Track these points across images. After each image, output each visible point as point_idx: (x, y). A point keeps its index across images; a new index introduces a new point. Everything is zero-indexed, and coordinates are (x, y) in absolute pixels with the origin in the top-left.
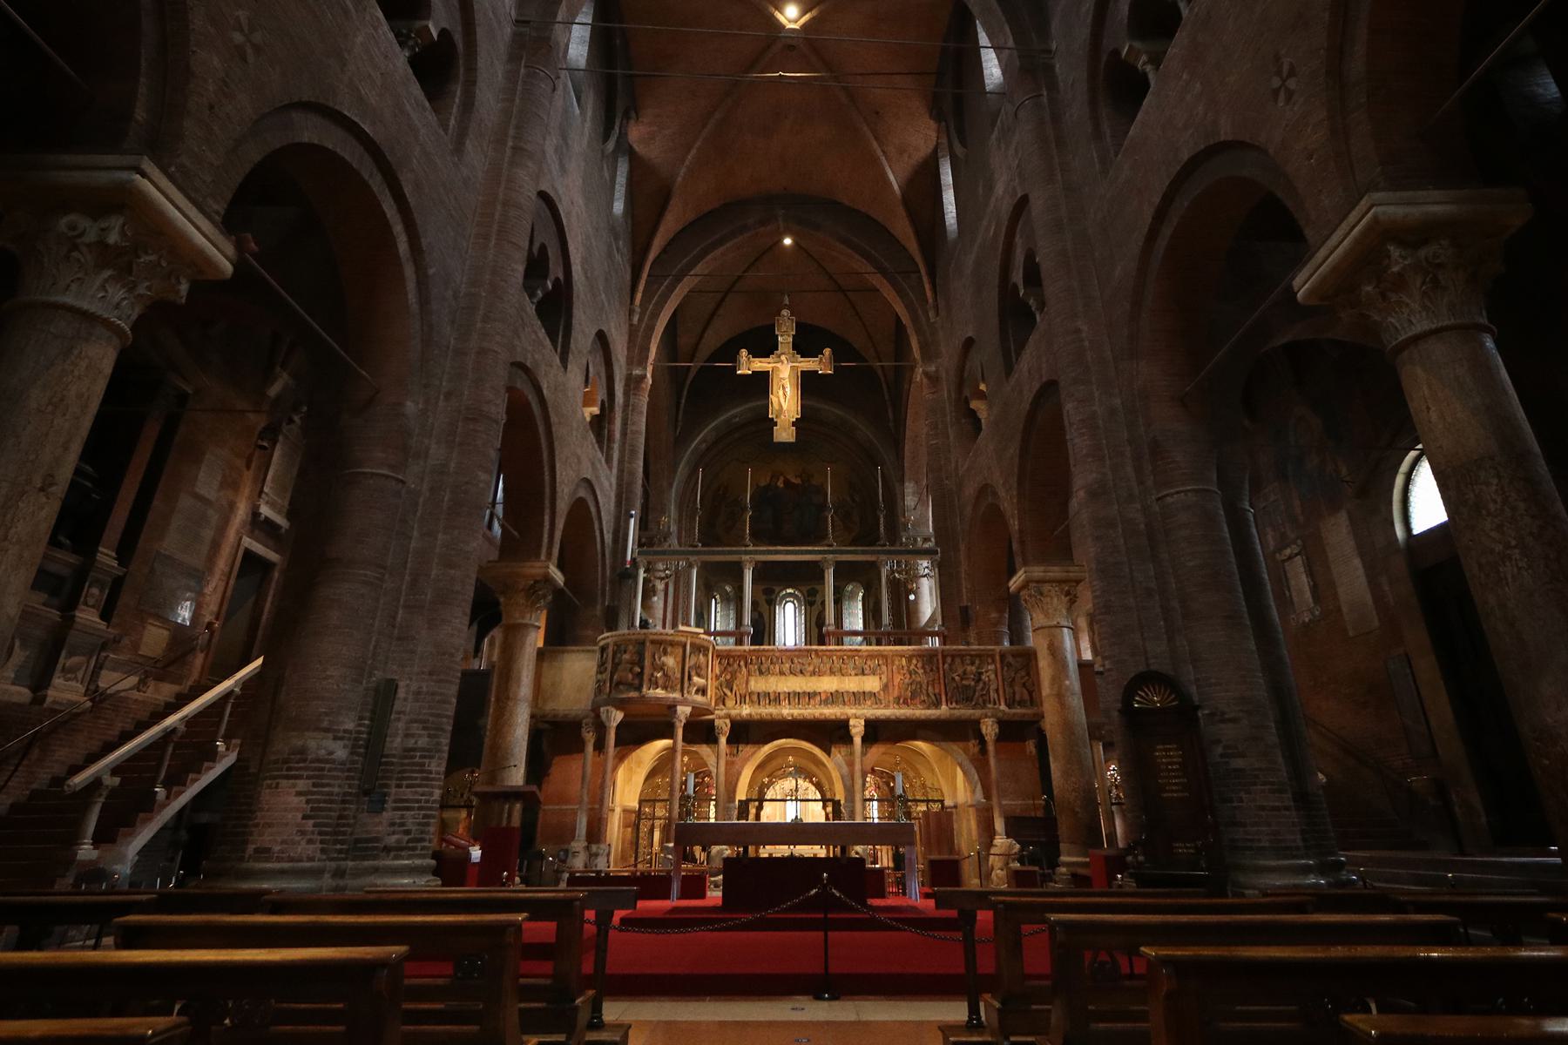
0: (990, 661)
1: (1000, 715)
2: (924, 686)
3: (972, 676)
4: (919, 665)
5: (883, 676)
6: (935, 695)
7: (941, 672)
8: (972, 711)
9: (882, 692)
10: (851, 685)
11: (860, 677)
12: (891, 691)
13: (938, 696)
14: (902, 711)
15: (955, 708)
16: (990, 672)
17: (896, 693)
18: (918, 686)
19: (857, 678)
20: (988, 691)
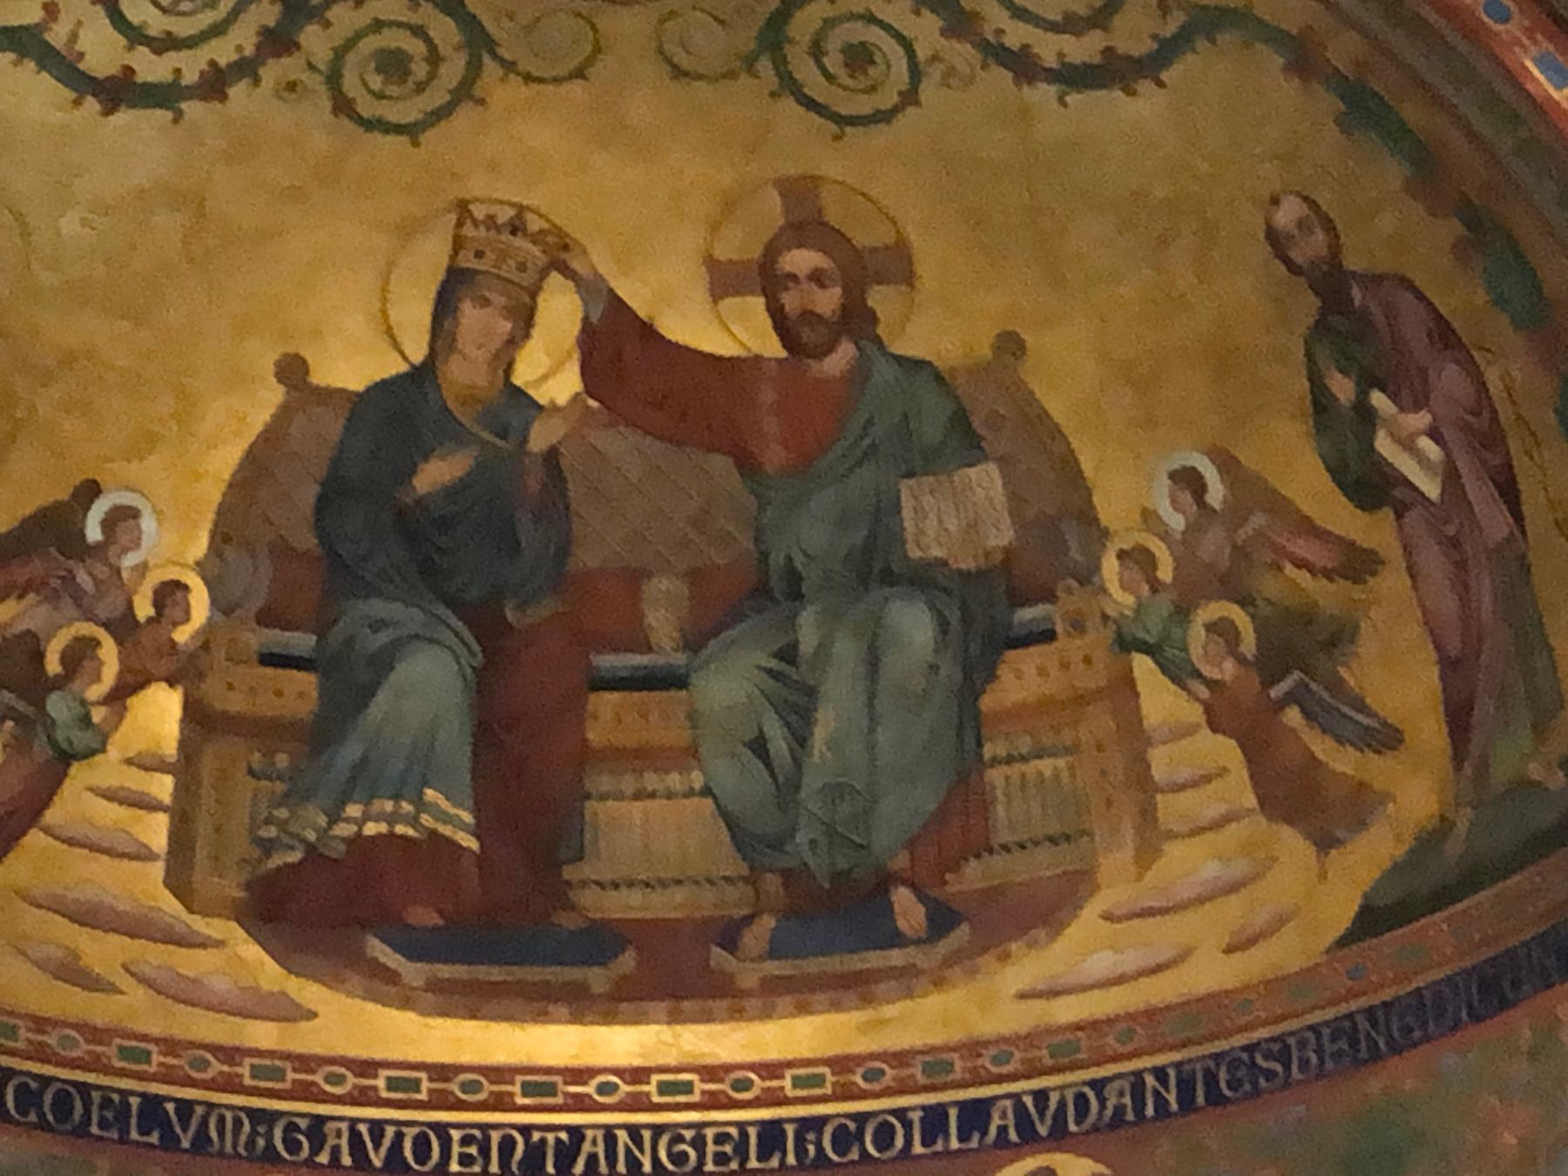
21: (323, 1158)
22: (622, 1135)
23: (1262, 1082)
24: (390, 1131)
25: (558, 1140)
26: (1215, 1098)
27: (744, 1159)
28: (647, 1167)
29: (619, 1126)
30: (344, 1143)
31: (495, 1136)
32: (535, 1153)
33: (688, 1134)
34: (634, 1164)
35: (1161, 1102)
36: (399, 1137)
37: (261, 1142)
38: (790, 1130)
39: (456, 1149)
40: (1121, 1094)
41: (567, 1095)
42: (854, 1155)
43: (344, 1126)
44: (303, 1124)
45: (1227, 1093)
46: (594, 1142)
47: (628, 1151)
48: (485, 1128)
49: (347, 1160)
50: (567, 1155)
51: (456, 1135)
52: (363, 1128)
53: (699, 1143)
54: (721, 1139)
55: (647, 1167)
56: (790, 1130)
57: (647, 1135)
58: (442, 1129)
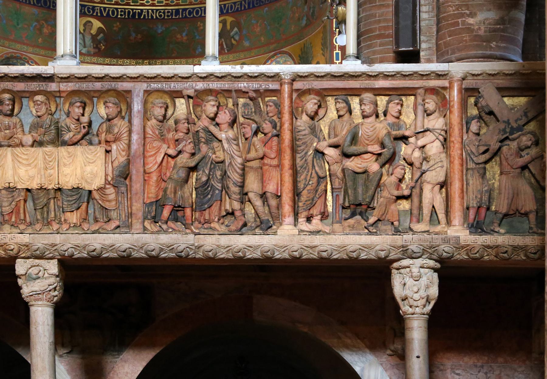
0: (431, 105)
1: (445, 249)
2: (235, 176)
3: (376, 148)
4: (224, 117)
5: (114, 147)
6: (263, 196)
7: (287, 136)
8: (365, 239)
9: (110, 190)
10: (22, 171)
11: (49, 149)
12: (137, 185)
13: (273, 202)
14: (164, 239)
15: (318, 232)
16: (429, 137)
17: (152, 193)
18: (218, 173)
19: (39, 152)
20: (418, 183)
21: (95, 14)
22: (150, 11)
23: (261, 4)
24: (107, 9)
25: (138, 12)
26: (254, 6)
27: (172, 16)
28: (155, 18)
29: (150, 9)
30: (99, 11)
31: (127, 11)
32: (134, 14)
33: (162, 11)
34: (152, 17)
35: (245, 7)
36: (109, 10)
37: (83, 10)
38: (181, 10)
39: (119, 13)
40: (238, 5)
41: (140, 3)
42: (192, 16)
43: (99, 8)
44: (91, 7)
45: (256, 6)
46: (145, 13)
47: (151, 14)
48: (125, 9)
49: (99, 14)
50: (140, 14)
51: (119, 10)
52: (102, 8)
53: (164, 13)
54: (168, 12)
55: (155, 18)
56: (181, 10)
57: (155, 11)
58: (117, 9)
